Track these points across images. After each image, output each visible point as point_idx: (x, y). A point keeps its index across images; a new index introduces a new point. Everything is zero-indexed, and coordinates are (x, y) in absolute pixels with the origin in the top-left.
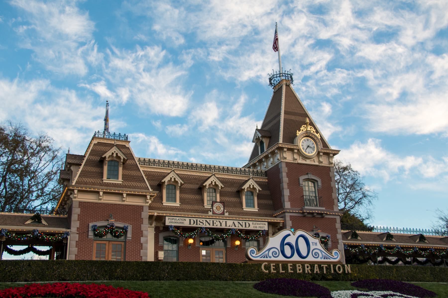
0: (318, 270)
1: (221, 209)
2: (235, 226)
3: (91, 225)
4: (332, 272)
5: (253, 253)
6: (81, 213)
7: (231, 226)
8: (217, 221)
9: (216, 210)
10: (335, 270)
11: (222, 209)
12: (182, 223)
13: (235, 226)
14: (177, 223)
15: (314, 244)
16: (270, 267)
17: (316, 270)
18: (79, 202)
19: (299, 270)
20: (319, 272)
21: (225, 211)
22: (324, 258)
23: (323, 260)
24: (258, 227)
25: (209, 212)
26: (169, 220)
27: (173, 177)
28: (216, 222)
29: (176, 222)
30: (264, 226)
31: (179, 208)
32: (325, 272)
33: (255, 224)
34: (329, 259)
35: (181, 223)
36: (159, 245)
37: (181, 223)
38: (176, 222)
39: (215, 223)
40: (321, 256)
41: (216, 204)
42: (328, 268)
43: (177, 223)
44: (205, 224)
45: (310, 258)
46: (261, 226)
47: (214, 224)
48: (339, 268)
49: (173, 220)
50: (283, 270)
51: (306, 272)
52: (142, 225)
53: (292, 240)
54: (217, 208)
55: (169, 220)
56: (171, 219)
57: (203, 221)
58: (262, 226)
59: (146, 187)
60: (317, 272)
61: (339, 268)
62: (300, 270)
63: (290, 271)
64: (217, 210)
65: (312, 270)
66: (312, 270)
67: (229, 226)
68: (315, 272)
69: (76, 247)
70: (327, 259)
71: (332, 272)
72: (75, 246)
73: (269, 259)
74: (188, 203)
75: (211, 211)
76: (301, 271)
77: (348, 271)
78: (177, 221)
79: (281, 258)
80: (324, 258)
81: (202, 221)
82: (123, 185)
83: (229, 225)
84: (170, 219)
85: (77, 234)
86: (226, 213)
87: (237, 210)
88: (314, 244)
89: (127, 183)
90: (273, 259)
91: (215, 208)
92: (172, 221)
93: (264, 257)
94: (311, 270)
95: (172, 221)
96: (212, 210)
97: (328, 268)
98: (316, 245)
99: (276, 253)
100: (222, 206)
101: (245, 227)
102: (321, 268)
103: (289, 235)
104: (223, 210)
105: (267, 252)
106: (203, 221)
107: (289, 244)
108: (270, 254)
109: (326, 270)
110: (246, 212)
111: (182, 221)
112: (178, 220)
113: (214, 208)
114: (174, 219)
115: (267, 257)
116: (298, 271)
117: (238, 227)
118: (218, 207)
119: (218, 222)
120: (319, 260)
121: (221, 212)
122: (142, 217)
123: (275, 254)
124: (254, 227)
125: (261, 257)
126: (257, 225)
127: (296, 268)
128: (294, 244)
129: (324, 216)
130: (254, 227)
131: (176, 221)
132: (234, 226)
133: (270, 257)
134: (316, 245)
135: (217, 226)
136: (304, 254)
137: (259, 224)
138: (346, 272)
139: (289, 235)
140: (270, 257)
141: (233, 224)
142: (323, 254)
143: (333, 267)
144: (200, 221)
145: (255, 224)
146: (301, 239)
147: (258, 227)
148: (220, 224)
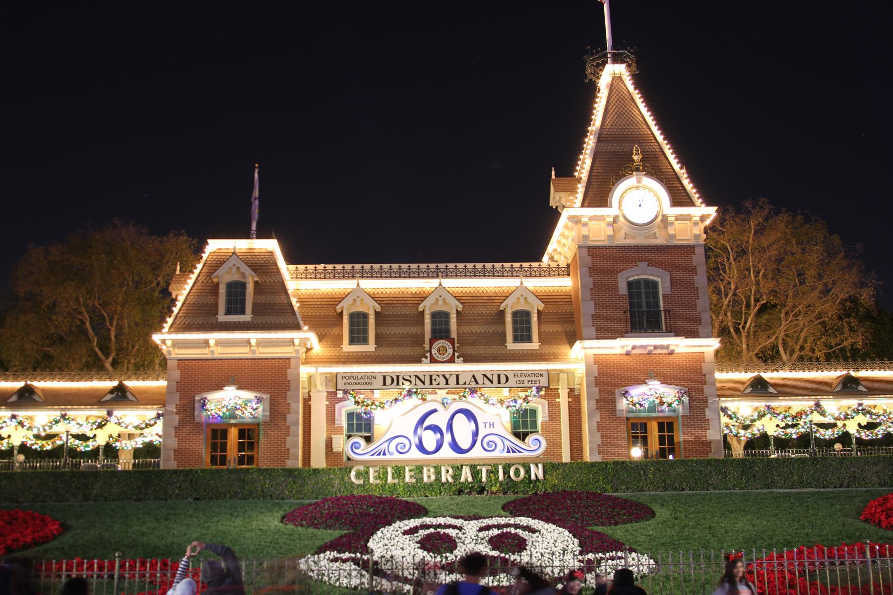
0: (469, 474)
1: (448, 351)
2: (477, 383)
3: (197, 398)
4: (501, 477)
5: (356, 448)
6: (181, 378)
7: (467, 383)
8: (438, 376)
9: (437, 353)
10: (506, 472)
11: (450, 351)
12: (369, 383)
13: (477, 383)
14: (359, 383)
15: (488, 425)
16: (367, 473)
17: (466, 474)
18: (179, 360)
19: (428, 476)
20: (470, 479)
21: (456, 354)
22: (508, 452)
23: (505, 454)
24: (526, 382)
25: (423, 359)
26: (344, 379)
27: (358, 297)
28: (437, 377)
29: (356, 384)
30: (539, 378)
31: (372, 354)
32: (484, 480)
33: (519, 376)
34: (520, 452)
35: (366, 383)
36: (336, 426)
37: (366, 383)
38: (356, 384)
39: (435, 380)
40: (500, 446)
41: (437, 342)
42: (493, 472)
43: (359, 383)
44: (413, 383)
45: (477, 453)
46: (534, 378)
47: (433, 381)
48: (517, 472)
49: (352, 379)
50: (393, 478)
51: (444, 480)
52: (288, 392)
53: (440, 419)
54: (439, 350)
55: (344, 379)
56: (347, 378)
57: (410, 376)
58: (536, 378)
59: (296, 323)
60: (466, 480)
61: (517, 472)
62: (429, 477)
63: (407, 479)
64: (440, 354)
65: (456, 477)
66: (456, 477)
67: (465, 384)
68: (462, 480)
69: (175, 437)
70: (514, 452)
71: (501, 477)
72: (173, 436)
73: (388, 457)
74: (393, 344)
75: (426, 358)
76: (433, 477)
77: (536, 476)
78: (359, 381)
79: (415, 454)
80: (508, 452)
81: (409, 378)
82: (253, 323)
83: (464, 382)
84: (345, 377)
85: (177, 414)
86: (458, 357)
87: (496, 350)
88: (488, 425)
89: (260, 320)
90: (397, 456)
91: (436, 351)
92: (349, 381)
93: (379, 454)
94: (452, 477)
95: (349, 381)
96: (428, 355)
97: (493, 472)
98: (492, 426)
99: (405, 446)
100: (451, 346)
101: (497, 382)
102: (475, 473)
103: (435, 411)
104: (451, 353)
105: (386, 445)
106: (410, 376)
107: (435, 429)
108: (392, 448)
109: (488, 476)
110: (512, 352)
111: (369, 381)
112: (362, 378)
113: (434, 351)
114: (353, 377)
115: (384, 454)
116: (425, 479)
117: (484, 384)
118: (441, 349)
119: (441, 376)
120: (496, 454)
121: (449, 358)
122: (288, 379)
123: (401, 448)
124: (518, 382)
125: (373, 455)
126: (524, 378)
127: (421, 472)
128: (444, 427)
129: (674, 350)
130: (518, 382)
131: (356, 381)
132: (474, 383)
133: (391, 454)
134: (492, 426)
135: (438, 384)
136: (464, 443)
137: (529, 375)
138: (533, 477)
139: (435, 411)
140: (391, 454)
141: (473, 380)
142: (507, 442)
143: (504, 468)
144: (405, 377)
145: (519, 376)
146: (460, 418)
147: (526, 382)
148: (445, 381)
